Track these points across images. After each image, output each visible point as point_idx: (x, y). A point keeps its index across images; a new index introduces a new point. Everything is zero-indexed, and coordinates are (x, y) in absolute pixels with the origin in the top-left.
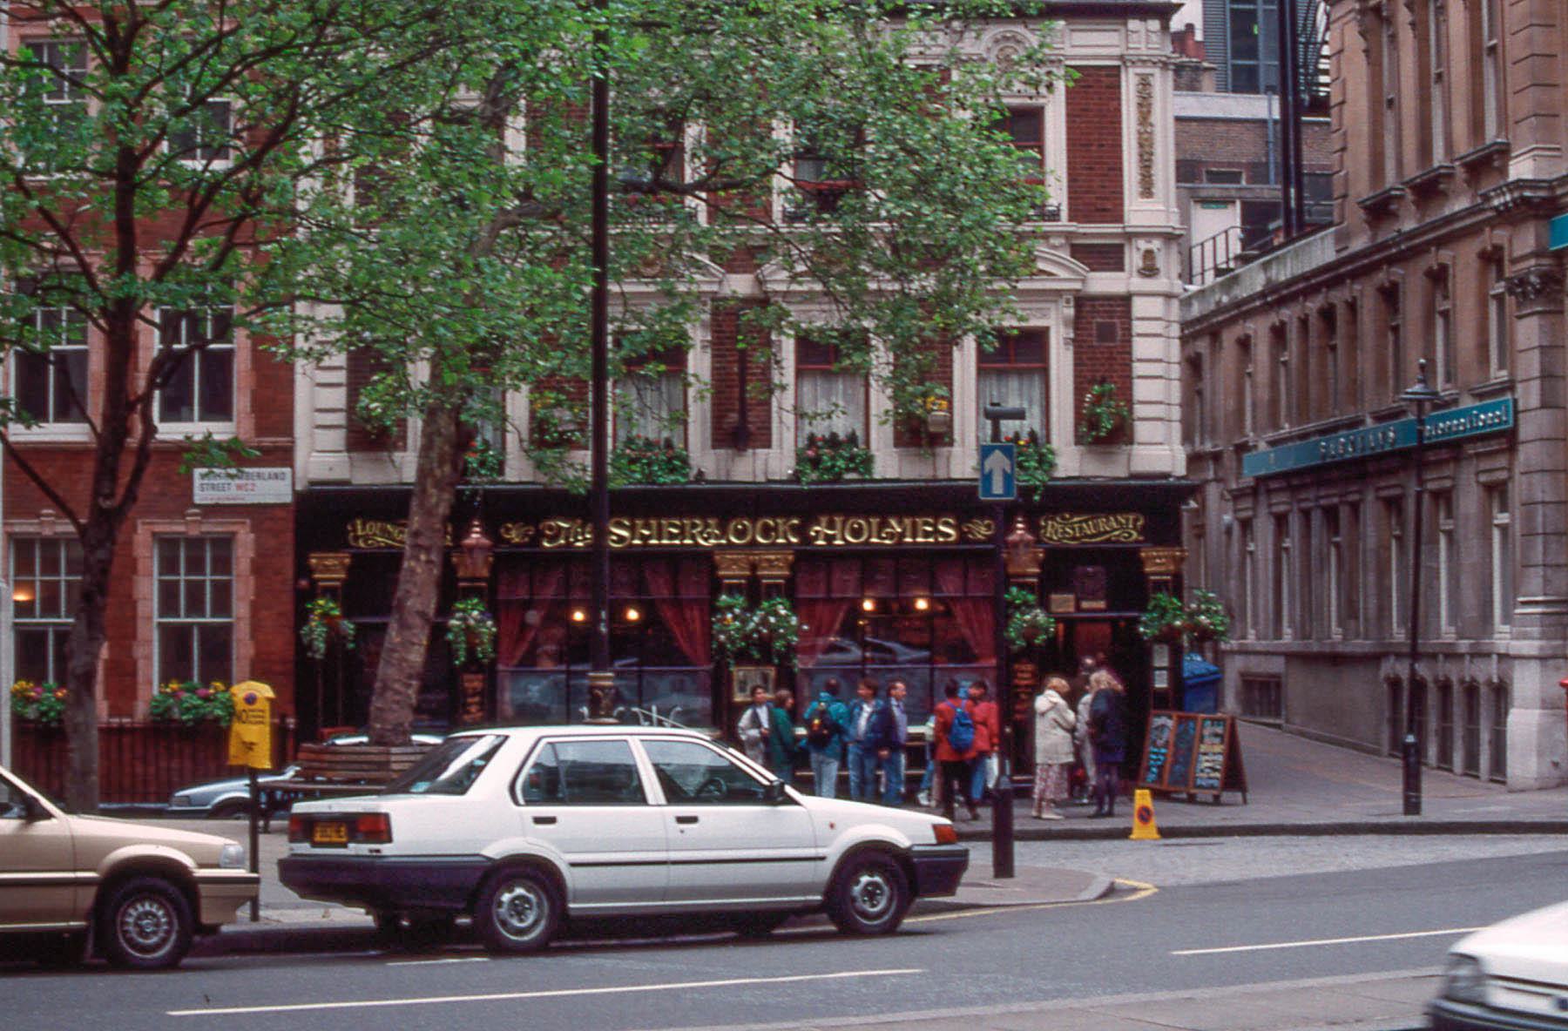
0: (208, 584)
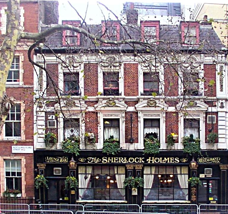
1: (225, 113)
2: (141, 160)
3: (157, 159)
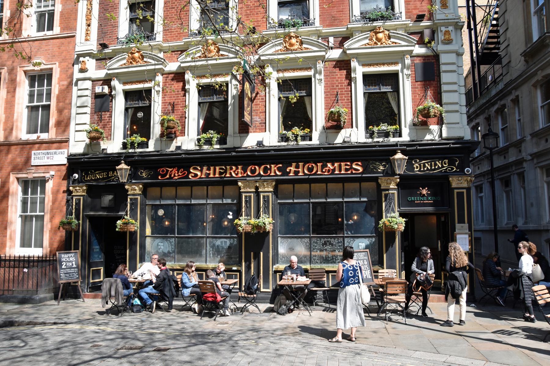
0: (38, 198)
1: (454, 55)
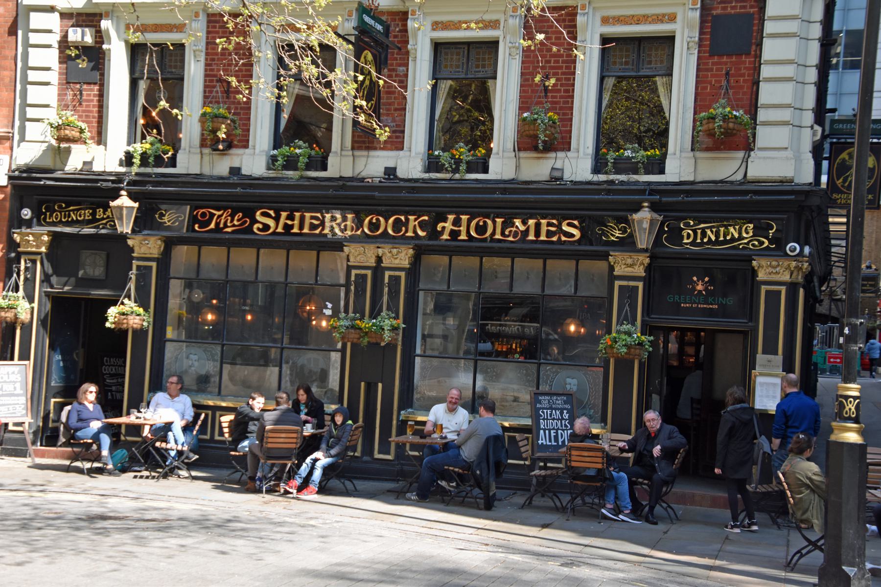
2: (415, 226)
3: (481, 223)
